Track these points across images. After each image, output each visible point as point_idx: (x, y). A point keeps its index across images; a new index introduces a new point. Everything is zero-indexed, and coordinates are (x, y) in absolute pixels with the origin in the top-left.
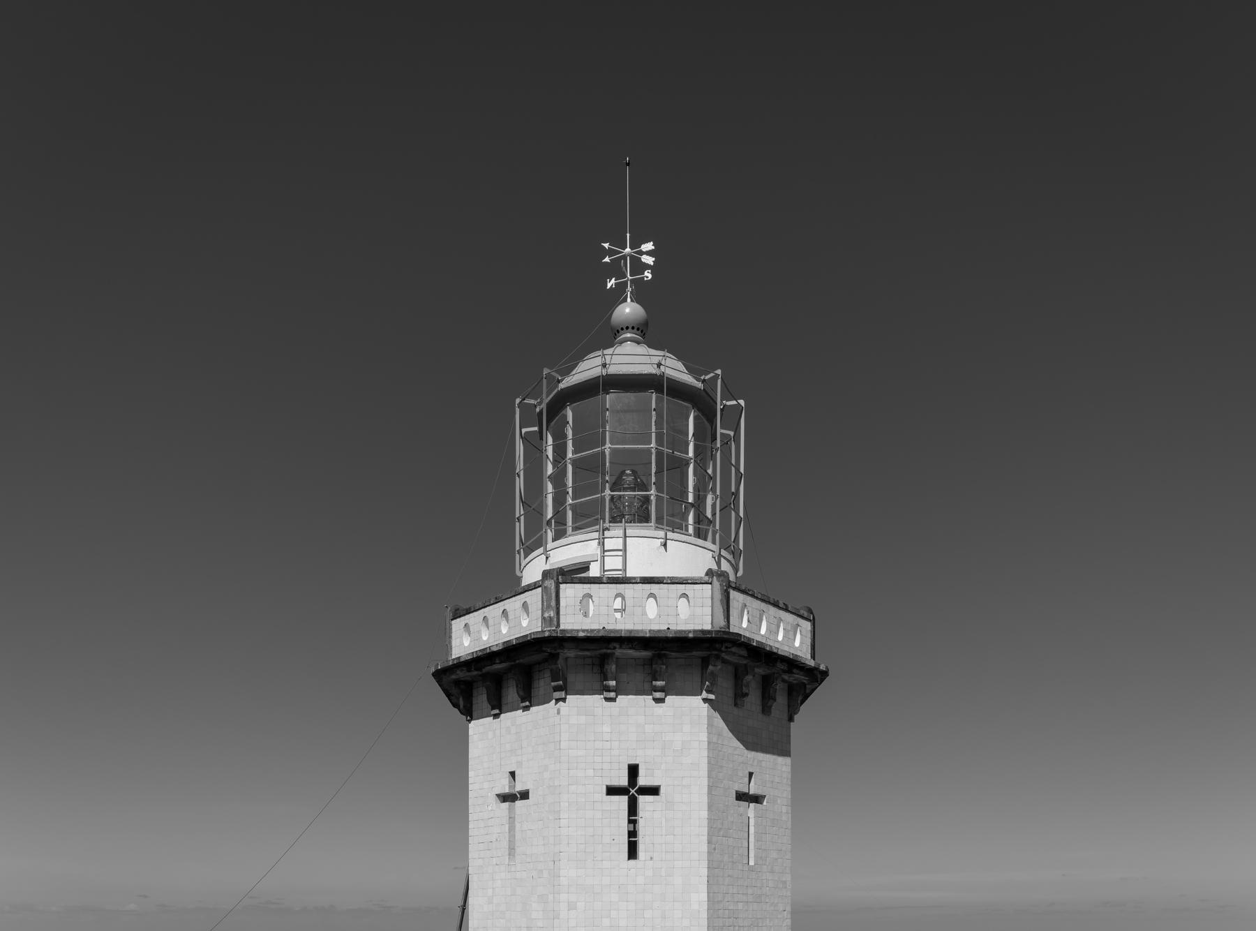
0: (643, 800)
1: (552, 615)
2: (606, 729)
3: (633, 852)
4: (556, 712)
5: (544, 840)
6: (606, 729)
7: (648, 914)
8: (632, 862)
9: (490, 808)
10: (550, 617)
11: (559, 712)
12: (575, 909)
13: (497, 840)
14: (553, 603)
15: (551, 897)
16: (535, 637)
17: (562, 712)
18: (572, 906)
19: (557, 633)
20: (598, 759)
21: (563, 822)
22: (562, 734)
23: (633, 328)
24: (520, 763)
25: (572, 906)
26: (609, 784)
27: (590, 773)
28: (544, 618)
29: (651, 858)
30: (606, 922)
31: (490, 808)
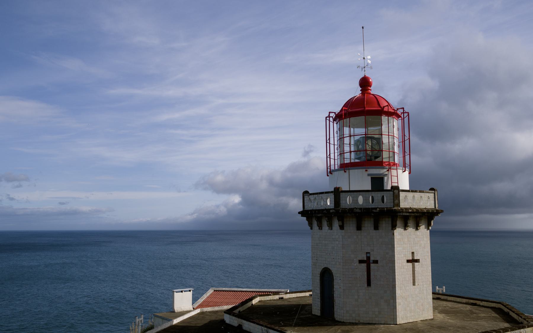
3: (414, 284)
9: (355, 265)
12: (400, 305)
24: (373, 250)
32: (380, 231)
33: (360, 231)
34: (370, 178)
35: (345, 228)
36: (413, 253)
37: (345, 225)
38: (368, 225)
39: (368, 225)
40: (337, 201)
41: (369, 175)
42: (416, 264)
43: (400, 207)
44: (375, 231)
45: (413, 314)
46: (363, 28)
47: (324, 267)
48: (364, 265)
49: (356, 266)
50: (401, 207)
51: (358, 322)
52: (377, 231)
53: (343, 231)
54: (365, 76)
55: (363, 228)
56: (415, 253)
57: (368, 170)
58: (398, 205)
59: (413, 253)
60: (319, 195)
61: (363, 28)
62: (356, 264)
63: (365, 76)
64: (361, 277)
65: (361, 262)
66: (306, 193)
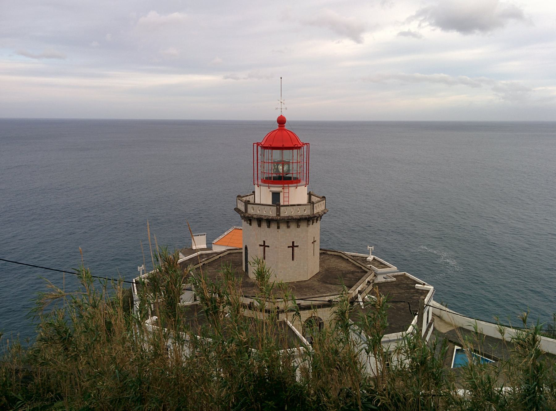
0: (295, 248)
2: (288, 234)
3: (293, 259)
7: (296, 272)
11: (278, 231)
18: (281, 272)
21: (279, 255)
24: (267, 240)
27: (285, 244)
28: (277, 214)
32: (271, 228)
34: (271, 193)
35: (252, 225)
37: (252, 223)
38: (264, 225)
39: (264, 225)
41: (270, 191)
44: (268, 229)
45: (291, 278)
46: (281, 78)
48: (262, 248)
53: (251, 227)
54: (281, 115)
55: (261, 226)
58: (279, 215)
61: (281, 78)
63: (281, 115)
65: (260, 245)
66: (239, 196)
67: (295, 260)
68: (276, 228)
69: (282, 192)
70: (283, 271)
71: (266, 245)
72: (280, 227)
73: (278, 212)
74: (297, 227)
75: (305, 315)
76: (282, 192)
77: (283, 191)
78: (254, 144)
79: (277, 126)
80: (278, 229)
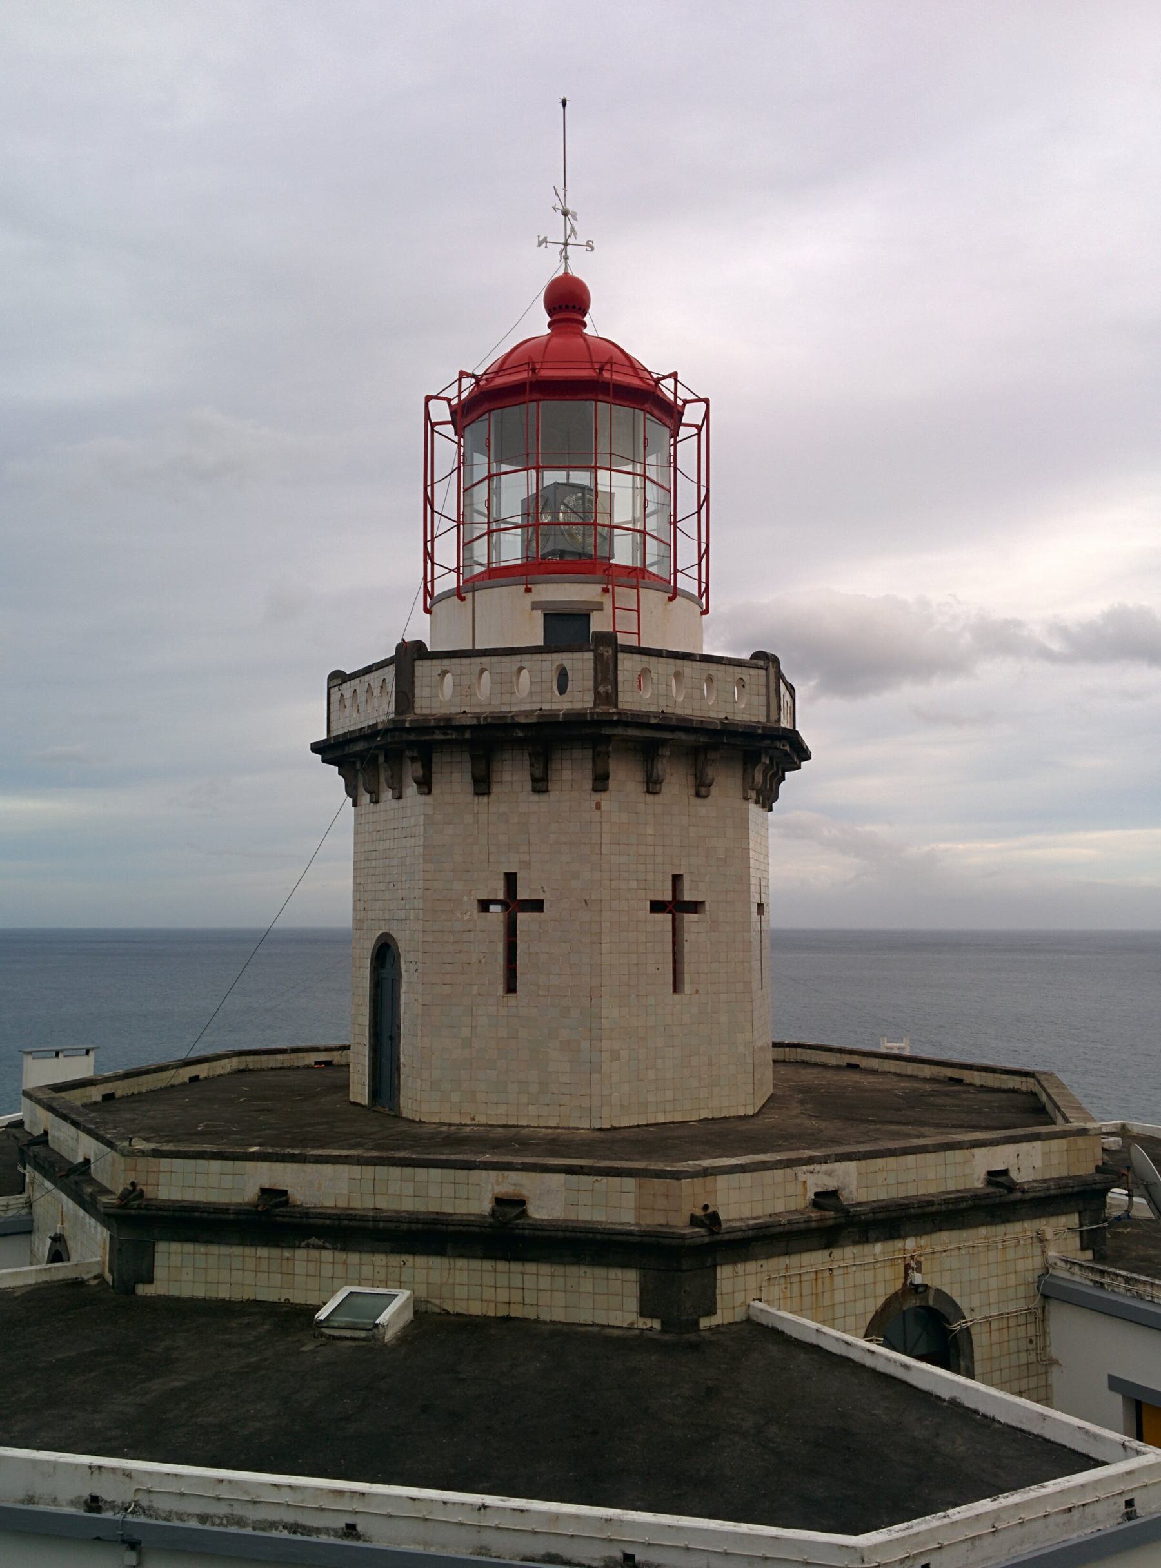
1: (610, 691)
3: (676, 987)
4: (594, 806)
5: (571, 968)
6: (650, 831)
8: (677, 997)
9: (466, 917)
10: (607, 693)
11: (598, 806)
12: (618, 1058)
13: (480, 961)
14: (611, 676)
15: (585, 1045)
16: (600, 718)
17: (603, 808)
19: (627, 717)
20: (641, 867)
21: (605, 948)
22: (603, 835)
23: (560, 307)
24: (527, 865)
25: (615, 1056)
26: (653, 899)
27: (633, 885)
29: (697, 990)
30: (651, 1074)
31: (466, 917)
32: (553, 796)
33: (485, 799)
34: (539, 615)
35: (436, 790)
36: (677, 879)
37: (435, 777)
40: (405, 695)
41: (535, 606)
42: (689, 918)
43: (616, 707)
44: (535, 797)
45: (669, 1095)
46: (564, 103)
47: (381, 932)
49: (469, 921)
50: (620, 706)
51: (469, 1122)
52: (544, 797)
53: (428, 799)
54: (566, 273)
55: (496, 789)
56: (686, 879)
57: (535, 588)
58: (611, 698)
59: (677, 879)
60: (362, 678)
61: (564, 103)
62: (469, 913)
63: (566, 273)
64: (483, 961)
66: (338, 678)
67: (688, 988)
68: (589, 785)
69: (599, 606)
70: (624, 1054)
71: (522, 895)
72: (612, 784)
73: (605, 680)
74: (692, 792)
75: (869, 1275)
76: (599, 606)
77: (608, 607)
78: (428, 398)
79: (539, 325)
80: (595, 790)
